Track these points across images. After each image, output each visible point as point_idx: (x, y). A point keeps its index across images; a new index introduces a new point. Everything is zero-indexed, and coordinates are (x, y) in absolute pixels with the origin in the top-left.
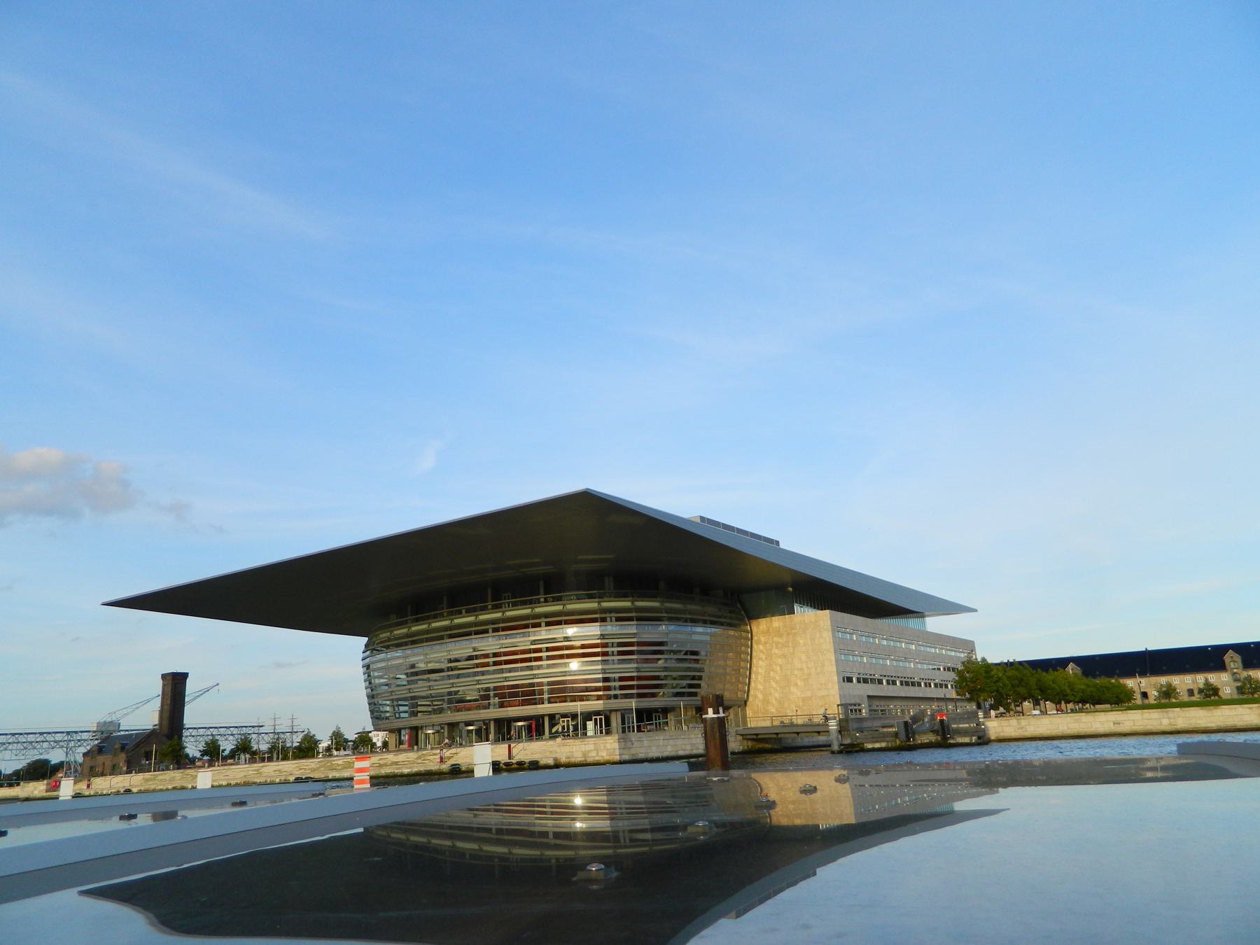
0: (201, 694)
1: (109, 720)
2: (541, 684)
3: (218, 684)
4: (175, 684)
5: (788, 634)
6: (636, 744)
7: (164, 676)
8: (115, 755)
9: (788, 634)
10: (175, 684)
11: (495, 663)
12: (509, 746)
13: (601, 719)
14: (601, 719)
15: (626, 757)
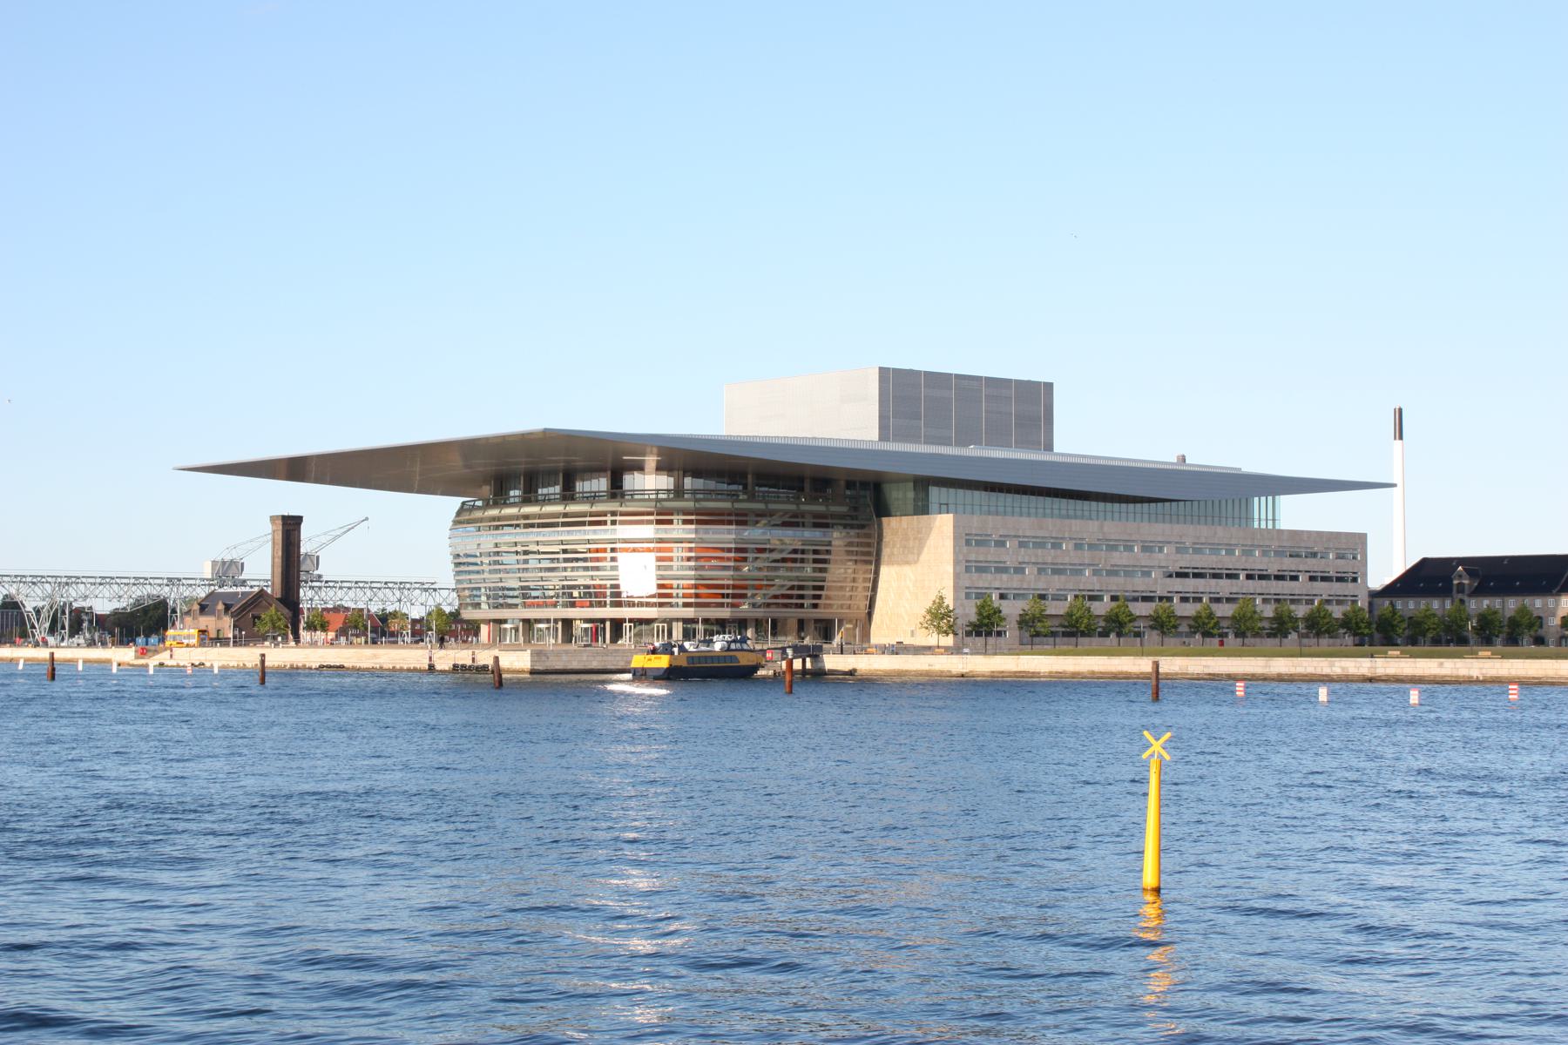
0: (345, 532)
1: (228, 558)
2: (605, 587)
3: (367, 519)
4: (290, 527)
5: (915, 539)
6: (551, 658)
7: (273, 519)
8: (219, 618)
9: (915, 539)
10: (290, 527)
11: (566, 560)
12: (473, 653)
13: (663, 627)
14: (663, 627)
15: (540, 667)
